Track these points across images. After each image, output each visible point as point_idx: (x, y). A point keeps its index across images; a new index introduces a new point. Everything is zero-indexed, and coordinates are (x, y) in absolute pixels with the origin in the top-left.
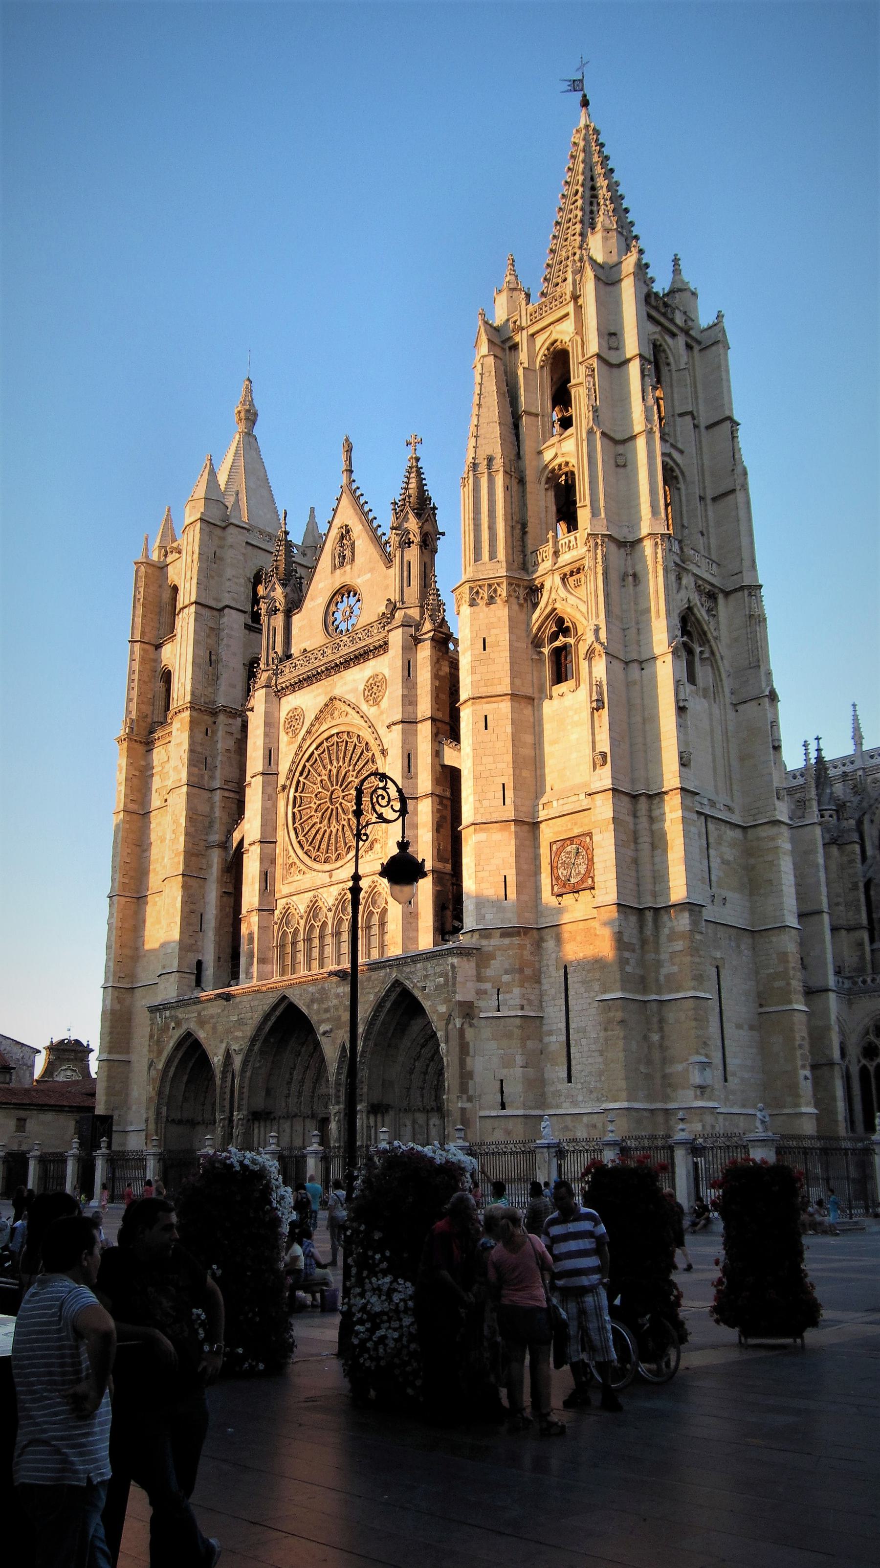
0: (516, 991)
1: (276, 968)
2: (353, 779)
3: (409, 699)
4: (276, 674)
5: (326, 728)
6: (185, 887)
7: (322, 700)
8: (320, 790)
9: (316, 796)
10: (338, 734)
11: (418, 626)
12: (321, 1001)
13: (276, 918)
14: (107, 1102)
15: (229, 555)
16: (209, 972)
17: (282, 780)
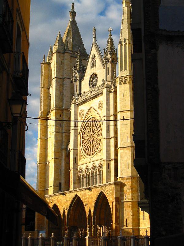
0: (131, 194)
1: (78, 185)
2: (96, 131)
3: (108, 109)
4: (77, 100)
5: (90, 116)
6: (55, 162)
7: (89, 108)
8: (88, 134)
9: (87, 136)
10: (92, 118)
11: (110, 87)
12: (85, 196)
13: (78, 171)
14: (38, 223)
15: (65, 61)
16: (63, 186)
17: (79, 131)
